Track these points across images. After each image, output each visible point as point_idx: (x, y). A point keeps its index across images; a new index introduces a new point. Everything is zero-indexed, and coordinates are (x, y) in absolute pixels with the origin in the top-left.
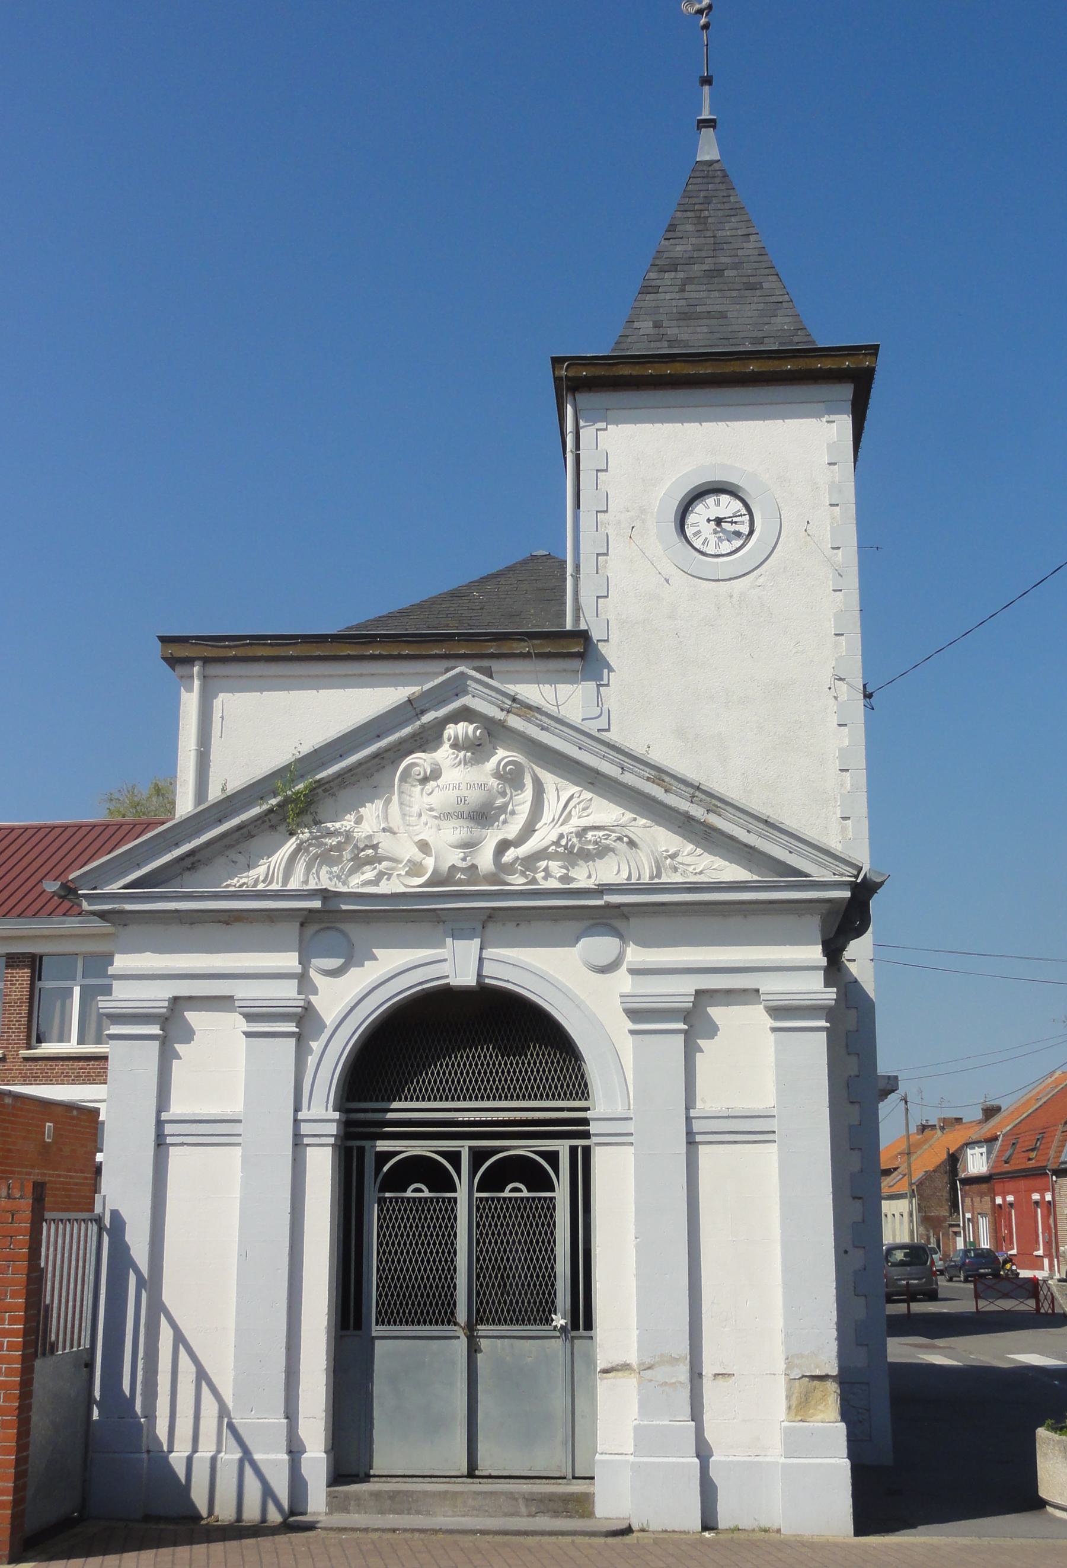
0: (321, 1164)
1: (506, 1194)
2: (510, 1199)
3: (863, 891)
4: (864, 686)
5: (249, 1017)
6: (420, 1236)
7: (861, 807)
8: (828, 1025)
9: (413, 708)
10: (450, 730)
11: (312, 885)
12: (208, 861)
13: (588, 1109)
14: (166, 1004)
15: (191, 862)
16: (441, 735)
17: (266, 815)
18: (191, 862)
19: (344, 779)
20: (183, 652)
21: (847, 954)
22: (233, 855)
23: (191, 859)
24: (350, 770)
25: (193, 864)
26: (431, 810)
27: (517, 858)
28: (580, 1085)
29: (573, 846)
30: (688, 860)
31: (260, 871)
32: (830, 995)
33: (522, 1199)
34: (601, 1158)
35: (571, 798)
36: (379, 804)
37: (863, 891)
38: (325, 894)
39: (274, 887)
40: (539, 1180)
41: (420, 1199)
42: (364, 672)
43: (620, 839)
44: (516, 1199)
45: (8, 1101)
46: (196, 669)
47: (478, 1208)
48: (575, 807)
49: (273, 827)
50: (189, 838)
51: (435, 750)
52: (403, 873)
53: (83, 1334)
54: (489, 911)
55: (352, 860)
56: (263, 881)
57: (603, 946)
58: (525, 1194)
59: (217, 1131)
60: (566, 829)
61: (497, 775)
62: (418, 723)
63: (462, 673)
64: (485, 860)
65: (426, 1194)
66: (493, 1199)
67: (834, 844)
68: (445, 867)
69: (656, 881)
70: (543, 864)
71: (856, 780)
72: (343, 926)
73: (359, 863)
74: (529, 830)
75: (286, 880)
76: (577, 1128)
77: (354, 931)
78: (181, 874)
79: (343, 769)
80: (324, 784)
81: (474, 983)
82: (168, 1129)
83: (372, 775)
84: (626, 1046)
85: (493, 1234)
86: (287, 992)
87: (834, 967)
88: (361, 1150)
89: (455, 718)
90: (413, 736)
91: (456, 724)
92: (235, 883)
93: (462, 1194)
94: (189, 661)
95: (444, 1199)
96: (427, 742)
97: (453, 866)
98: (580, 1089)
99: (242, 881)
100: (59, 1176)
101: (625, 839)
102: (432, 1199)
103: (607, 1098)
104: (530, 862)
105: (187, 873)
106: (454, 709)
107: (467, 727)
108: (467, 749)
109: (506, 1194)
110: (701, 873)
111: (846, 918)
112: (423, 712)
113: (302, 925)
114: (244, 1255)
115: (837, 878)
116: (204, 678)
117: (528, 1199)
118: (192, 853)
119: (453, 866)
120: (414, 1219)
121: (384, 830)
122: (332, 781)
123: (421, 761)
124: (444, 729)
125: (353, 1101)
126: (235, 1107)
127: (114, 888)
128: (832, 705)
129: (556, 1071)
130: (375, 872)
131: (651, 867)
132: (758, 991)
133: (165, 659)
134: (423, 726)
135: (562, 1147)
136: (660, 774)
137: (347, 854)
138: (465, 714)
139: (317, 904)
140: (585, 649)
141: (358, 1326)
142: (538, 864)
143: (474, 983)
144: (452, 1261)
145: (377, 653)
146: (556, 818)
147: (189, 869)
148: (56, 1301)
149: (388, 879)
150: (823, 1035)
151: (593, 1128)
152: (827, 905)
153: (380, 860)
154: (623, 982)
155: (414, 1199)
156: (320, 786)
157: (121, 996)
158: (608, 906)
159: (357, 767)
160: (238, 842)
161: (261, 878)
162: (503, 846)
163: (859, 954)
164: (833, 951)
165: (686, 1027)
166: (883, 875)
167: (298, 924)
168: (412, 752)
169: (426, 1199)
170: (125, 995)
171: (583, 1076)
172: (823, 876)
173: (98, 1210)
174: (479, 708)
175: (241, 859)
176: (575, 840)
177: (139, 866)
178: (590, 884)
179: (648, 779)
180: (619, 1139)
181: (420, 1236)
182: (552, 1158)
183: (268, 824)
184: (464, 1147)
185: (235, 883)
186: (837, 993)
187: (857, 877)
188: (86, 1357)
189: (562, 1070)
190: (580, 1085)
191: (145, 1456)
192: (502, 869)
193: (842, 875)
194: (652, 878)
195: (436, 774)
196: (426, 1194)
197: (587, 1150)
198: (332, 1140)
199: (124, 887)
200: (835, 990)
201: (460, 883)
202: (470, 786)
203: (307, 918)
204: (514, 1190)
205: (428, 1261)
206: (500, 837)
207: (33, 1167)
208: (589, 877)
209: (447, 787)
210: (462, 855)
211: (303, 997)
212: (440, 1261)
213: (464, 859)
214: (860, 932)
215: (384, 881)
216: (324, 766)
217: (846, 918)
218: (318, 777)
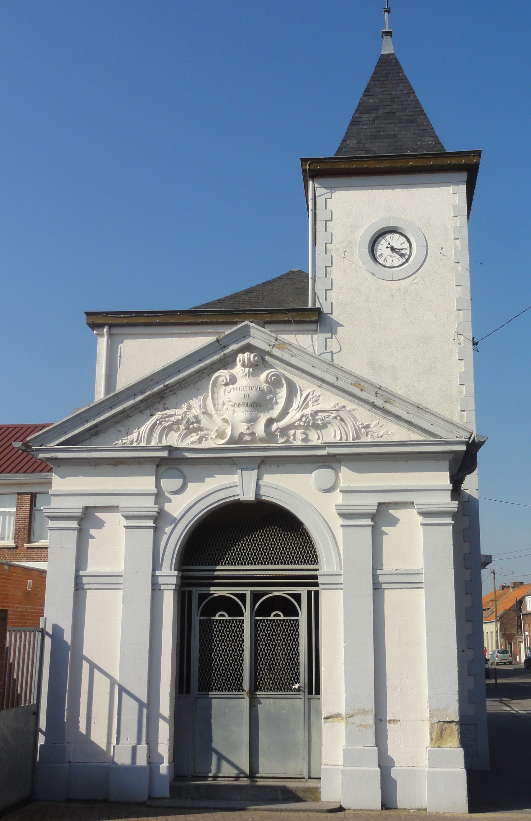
0: (169, 600)
1: (272, 617)
2: (274, 620)
4: (473, 338)
5: (127, 517)
6: (223, 641)
7: (471, 405)
8: (453, 522)
9: (220, 344)
10: (240, 356)
11: (164, 443)
12: (105, 430)
13: (318, 570)
14: (81, 510)
15: (95, 432)
16: (236, 360)
17: (138, 404)
18: (95, 432)
19: (182, 384)
20: (97, 320)
21: (463, 486)
22: (119, 427)
23: (96, 430)
24: (184, 379)
25: (97, 432)
26: (230, 401)
27: (278, 428)
28: (313, 557)
29: (309, 422)
30: (375, 429)
31: (134, 436)
32: (454, 506)
33: (280, 620)
34: (324, 596)
35: (308, 395)
36: (201, 398)
38: (170, 449)
39: (142, 444)
41: (223, 620)
42: (197, 331)
43: (335, 418)
44: (277, 620)
45: (6, 567)
47: (255, 625)
48: (310, 400)
49: (141, 412)
50: (94, 418)
51: (233, 367)
52: (214, 437)
53: (32, 696)
55: (185, 429)
56: (136, 442)
57: (323, 475)
58: (282, 617)
59: (109, 582)
60: (305, 412)
61: (267, 382)
62: (223, 353)
63: (247, 325)
64: (260, 429)
65: (227, 617)
66: (264, 620)
67: (456, 420)
68: (237, 435)
69: (357, 441)
70: (292, 432)
71: (467, 391)
73: (189, 431)
74: (285, 413)
75: (149, 440)
76: (311, 581)
77: (185, 469)
78: (90, 438)
79: (180, 379)
80: (169, 388)
81: (253, 499)
82: (85, 580)
83: (197, 382)
84: (339, 533)
85: (264, 640)
86: (148, 504)
87: (456, 492)
88: (190, 593)
89: (242, 350)
90: (220, 360)
91: (244, 353)
92: (119, 443)
93: (247, 618)
94: (102, 326)
95: (236, 620)
96: (228, 364)
98: (314, 559)
99: (124, 441)
100: (35, 609)
101: (338, 418)
102: (230, 620)
103: (327, 564)
104: (284, 431)
105: (94, 438)
106: (243, 345)
107: (250, 355)
108: (250, 367)
109: (272, 617)
110: (381, 437)
111: (463, 463)
112: (225, 347)
114: (124, 651)
115: (458, 439)
116: (110, 335)
117: (284, 620)
118: (96, 426)
119: (242, 433)
120: (220, 631)
121: (204, 413)
123: (223, 374)
124: (237, 356)
125: (186, 565)
126: (120, 568)
127: (52, 445)
128: (456, 348)
129: (299, 548)
130: (198, 436)
131: (353, 434)
132: (413, 503)
133: (89, 325)
135: (303, 591)
136: (359, 382)
137: (182, 427)
138: (249, 348)
139: (165, 454)
140: (319, 318)
141: (188, 692)
142: (290, 432)
143: (253, 499)
144: (241, 655)
145: (205, 320)
146: (300, 406)
147: (94, 435)
148: (20, 677)
149: (206, 440)
150: (450, 528)
151: (320, 580)
152: (452, 456)
153: (201, 430)
154: (338, 497)
155: (220, 620)
156: (168, 388)
157: (56, 506)
158: (329, 456)
161: (135, 440)
162: (270, 422)
163: (471, 484)
164: (457, 480)
165: (373, 523)
167: (155, 466)
169: (226, 620)
170: (58, 505)
171: (315, 552)
172: (450, 438)
173: (42, 626)
174: (256, 345)
175: (123, 429)
176: (310, 418)
177: (66, 433)
178: (319, 443)
179: (351, 384)
180: (334, 586)
181: (223, 641)
182: (297, 597)
184: (248, 591)
185: (119, 443)
186: (458, 505)
187: (469, 438)
188: (34, 709)
189: (303, 548)
190: (313, 557)
191: (67, 765)
192: (270, 435)
193: (461, 437)
194: (353, 439)
195: (233, 380)
196: (227, 617)
197: (317, 593)
198: (173, 587)
199: (58, 445)
200: (457, 502)
201: (246, 442)
202: (251, 388)
203: (160, 462)
204: (275, 615)
205: (228, 655)
206: (268, 417)
207: (20, 604)
208: (319, 438)
210: (246, 427)
211: (157, 506)
212: (234, 655)
213: (248, 429)
214: (471, 471)
215: (203, 442)
216: (169, 377)
217: (463, 463)
218: (166, 383)
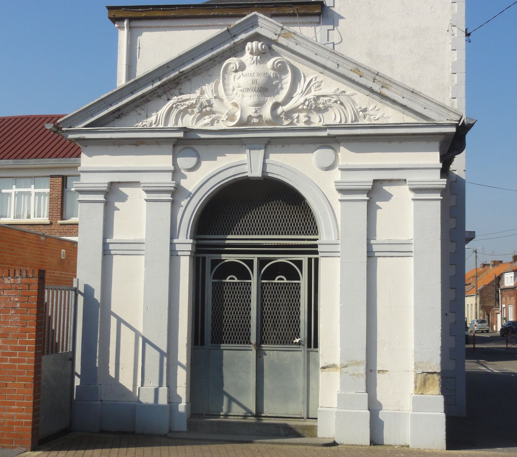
0: (185, 264)
1: (276, 281)
2: (278, 283)
3: (463, 129)
4: (466, 30)
5: (147, 192)
6: (233, 301)
8: (442, 198)
9: (231, 34)
10: (249, 45)
11: (180, 125)
13: (318, 239)
14: (107, 185)
15: (118, 115)
16: (245, 48)
17: (156, 90)
19: (196, 71)
20: (117, 15)
21: (452, 167)
22: (139, 110)
23: (118, 113)
25: (119, 115)
26: (239, 87)
27: (283, 111)
28: (313, 228)
29: (311, 106)
30: (372, 113)
31: (153, 118)
32: (443, 183)
33: (284, 283)
34: (322, 263)
35: (311, 81)
36: (213, 84)
37: (463, 129)
38: (185, 130)
39: (160, 126)
40: (291, 272)
41: (233, 283)
42: (209, 24)
43: (336, 102)
44: (281, 283)
45: (43, 238)
46: (125, 23)
47: (261, 288)
48: (313, 85)
49: (159, 96)
51: (242, 55)
52: (225, 120)
53: (68, 345)
54: (269, 139)
55: (199, 112)
56: (155, 124)
57: (324, 155)
58: (285, 281)
59: (133, 248)
61: (273, 68)
62: (233, 42)
63: (255, 16)
64: (266, 113)
65: (236, 280)
66: (269, 283)
67: (448, 104)
68: (245, 117)
69: (355, 123)
70: (295, 115)
71: (460, 79)
72: (197, 147)
73: (202, 114)
74: (289, 97)
75: (166, 123)
76: (312, 249)
77: (201, 149)
78: (113, 120)
79: (194, 66)
80: (184, 74)
81: (260, 176)
82: (111, 247)
83: (209, 69)
84: (338, 207)
85: (269, 301)
86: (167, 180)
87: (445, 172)
88: (204, 259)
89: (251, 39)
91: (252, 42)
93: (254, 281)
94: (122, 19)
95: (245, 283)
96: (237, 52)
97: (250, 116)
98: (315, 230)
99: (144, 124)
100: (69, 275)
101: (339, 102)
102: (239, 283)
103: (327, 234)
104: (288, 114)
105: (117, 120)
106: (251, 34)
107: (258, 44)
108: (258, 55)
109: (276, 281)
110: (378, 119)
111: (453, 143)
112: (235, 36)
113: (174, 146)
114: (146, 308)
116: (130, 28)
117: (287, 283)
118: (118, 109)
119: (250, 116)
120: (230, 292)
121: (215, 98)
122: (189, 72)
123: (233, 62)
124: (246, 45)
125: (200, 234)
126: (142, 236)
127: (80, 127)
128: (449, 39)
129: (301, 220)
130: (211, 119)
131: (352, 117)
132: (405, 180)
133: (111, 18)
134: (235, 43)
135: (304, 258)
136: (358, 68)
137: (196, 110)
138: (257, 37)
139: (181, 135)
140: (321, 11)
141: (202, 344)
142: (294, 115)
143: (260, 176)
144: (249, 313)
145: (216, 14)
147: (117, 118)
148: (57, 328)
149: (217, 123)
150: (439, 203)
151: (319, 249)
152: (443, 137)
153: (213, 113)
154: (337, 175)
155: (230, 283)
156: (183, 75)
157: (85, 182)
158: (329, 137)
159: (201, 65)
160: (141, 104)
162: (276, 106)
163: (459, 164)
164: (446, 161)
165: (368, 198)
166: (473, 120)
167: (171, 146)
168: (230, 57)
169: (236, 283)
170: (87, 180)
171: (315, 223)
173: (75, 285)
174: (263, 34)
175: (142, 112)
176: (313, 102)
177: (92, 116)
178: (320, 125)
179: (351, 70)
180: (332, 254)
181: (233, 301)
182: (299, 263)
183: (156, 95)
184: (255, 258)
185: (140, 125)
186: (447, 182)
187: (459, 121)
188: (70, 356)
189: (304, 220)
190: (313, 228)
191: (99, 403)
192: (276, 118)
193: (451, 120)
194: (352, 122)
195: (242, 67)
196: (236, 280)
197: (317, 260)
198: (189, 253)
199: (85, 127)
200: (446, 180)
201: (254, 124)
202: (259, 74)
203: (176, 143)
204: (279, 279)
205: (237, 313)
206: (274, 101)
207: (56, 270)
208: (320, 121)
209: (247, 75)
210: (254, 110)
211: (174, 182)
212: (243, 313)
213: (256, 112)
215: (215, 124)
216: (184, 64)
217: (453, 143)
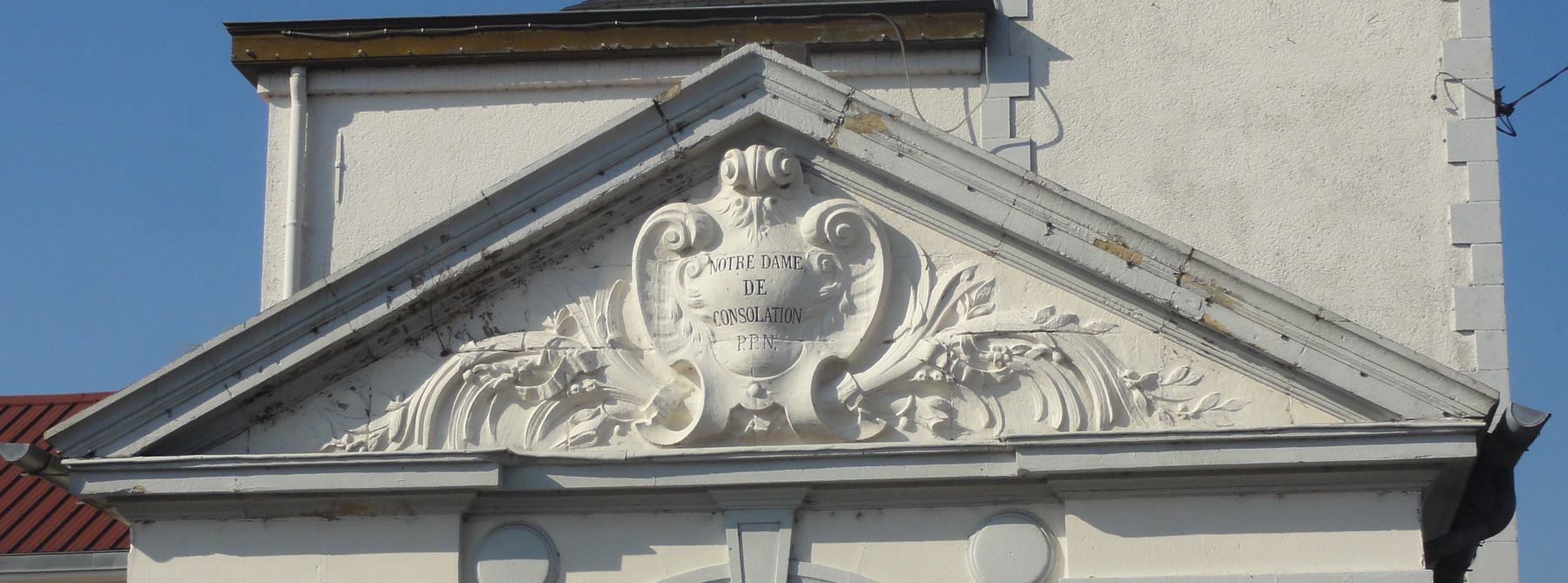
3: (1502, 447)
4: (1498, 93)
7: (1495, 312)
9: (665, 120)
10: (732, 158)
11: (487, 443)
12: (295, 405)
15: (265, 407)
16: (716, 170)
17: (399, 319)
18: (265, 407)
19: (544, 253)
20: (264, 52)
22: (340, 393)
23: (264, 402)
24: (551, 234)
25: (268, 409)
26: (699, 305)
27: (858, 391)
29: (959, 370)
30: (1174, 392)
31: (390, 420)
35: (955, 281)
36: (605, 297)
37: (1502, 447)
38: (506, 461)
39: (415, 448)
43: (1045, 355)
46: (293, 80)
48: (962, 298)
49: (413, 342)
50: (258, 363)
52: (649, 422)
54: (806, 490)
55: (554, 398)
56: (394, 440)
60: (945, 337)
61: (819, 239)
62: (674, 148)
63: (753, 56)
64: (798, 395)
67: (1444, 356)
69: (1116, 430)
70: (903, 404)
71: (1482, 263)
72: (543, 521)
73: (567, 405)
74: (878, 340)
75: (437, 435)
77: (559, 528)
79: (538, 233)
80: (502, 262)
83: (591, 245)
89: (738, 137)
90: (665, 172)
91: (743, 148)
92: (342, 444)
94: (279, 69)
97: (739, 407)
99: (357, 439)
101: (1055, 355)
104: (877, 400)
105: (259, 427)
106: (739, 122)
107: (763, 155)
108: (764, 194)
110: (1197, 415)
112: (682, 128)
113: (466, 518)
115: (1449, 422)
116: (310, 98)
119: (739, 407)
121: (614, 344)
122: (519, 255)
123: (676, 217)
124: (720, 158)
127: (125, 453)
128: (1439, 126)
130: (598, 420)
133: (240, 65)
134: (681, 154)
136: (1122, 236)
137: (545, 390)
138: (760, 131)
139: (489, 478)
140: (986, 32)
145: (615, 46)
146: (929, 317)
147: (261, 420)
149: (622, 433)
152: (1432, 475)
153: (605, 397)
156: (497, 265)
159: (563, 230)
160: (349, 369)
161: (391, 435)
162: (831, 371)
166: (1536, 413)
168: (663, 202)
172: (1423, 419)
175: (352, 399)
176: (963, 357)
177: (170, 414)
178: (991, 437)
179: (1096, 243)
183: (402, 336)
185: (342, 444)
192: (832, 414)
193: (1460, 416)
194: (1104, 425)
195: (709, 235)
199: (145, 452)
201: (753, 437)
202: (769, 262)
206: (824, 354)
208: (991, 423)
209: (726, 263)
210: (753, 388)
213: (760, 394)
214: (1495, 522)
216: (501, 228)
218: (492, 249)
